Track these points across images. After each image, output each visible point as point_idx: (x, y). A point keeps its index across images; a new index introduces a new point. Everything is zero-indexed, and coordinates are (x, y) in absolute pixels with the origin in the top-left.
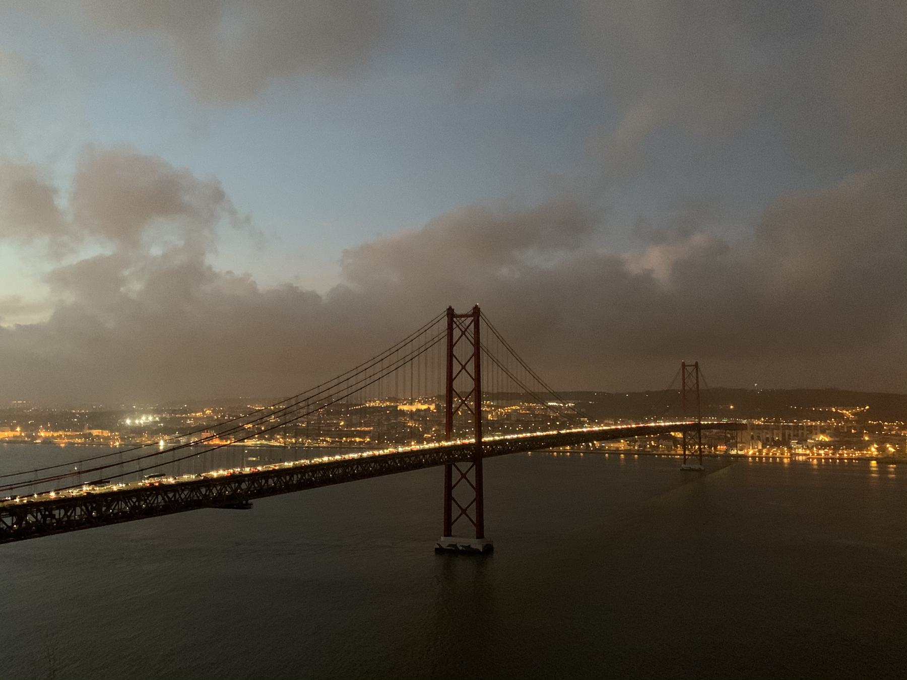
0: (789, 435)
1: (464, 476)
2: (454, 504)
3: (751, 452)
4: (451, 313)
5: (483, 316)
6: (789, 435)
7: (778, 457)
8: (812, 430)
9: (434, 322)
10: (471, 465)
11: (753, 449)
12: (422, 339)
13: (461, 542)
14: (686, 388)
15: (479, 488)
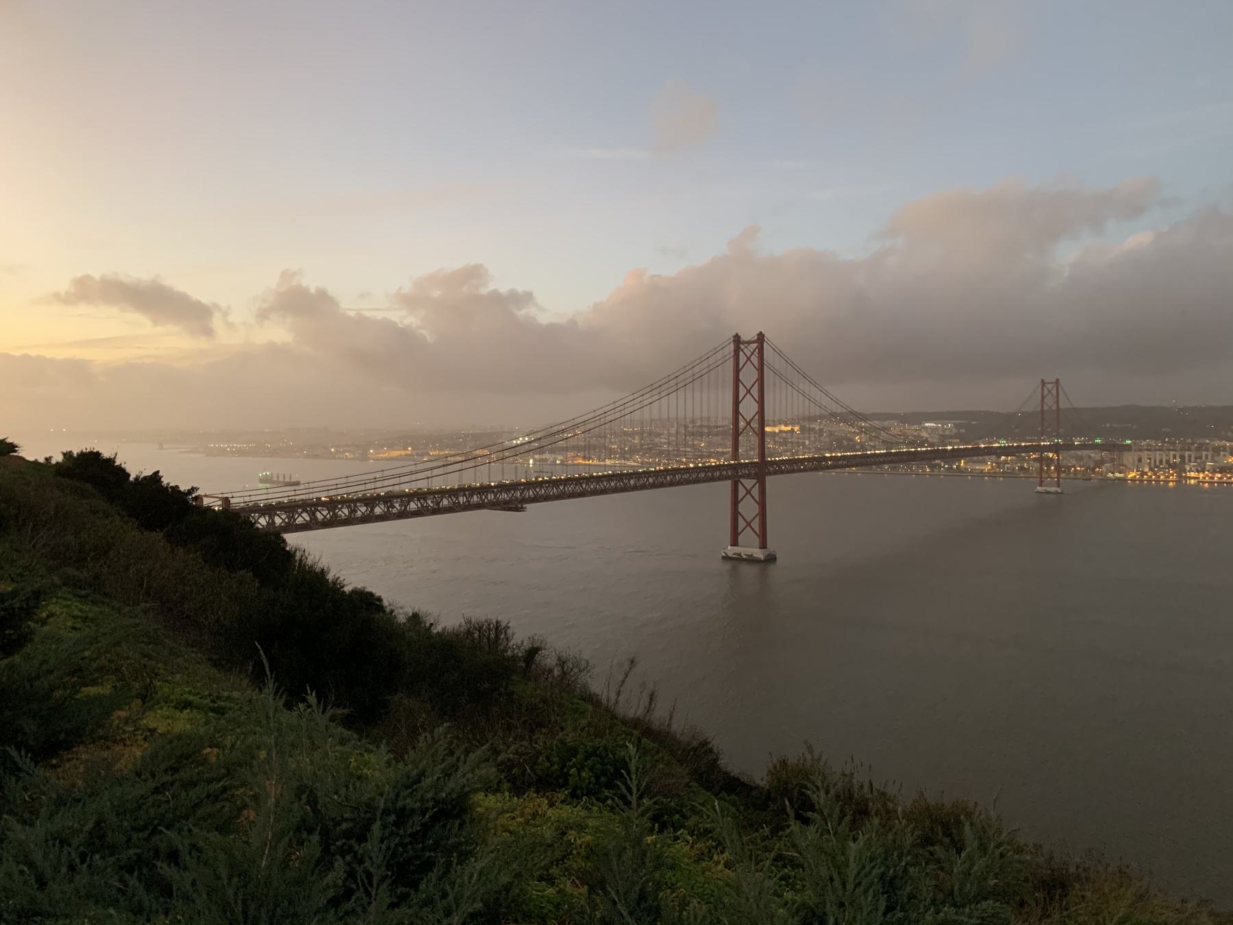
0: (1190, 456)
1: (749, 492)
2: (740, 517)
3: (1131, 475)
4: (737, 340)
5: (769, 342)
6: (1190, 456)
7: (1163, 481)
8: (1217, 450)
9: (718, 349)
10: (754, 483)
11: (1137, 471)
12: (705, 364)
13: (744, 551)
14: (1046, 408)
15: (762, 504)
